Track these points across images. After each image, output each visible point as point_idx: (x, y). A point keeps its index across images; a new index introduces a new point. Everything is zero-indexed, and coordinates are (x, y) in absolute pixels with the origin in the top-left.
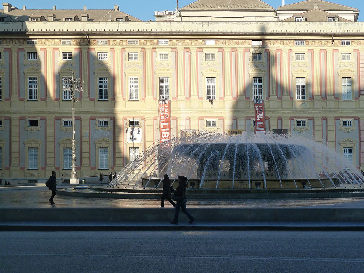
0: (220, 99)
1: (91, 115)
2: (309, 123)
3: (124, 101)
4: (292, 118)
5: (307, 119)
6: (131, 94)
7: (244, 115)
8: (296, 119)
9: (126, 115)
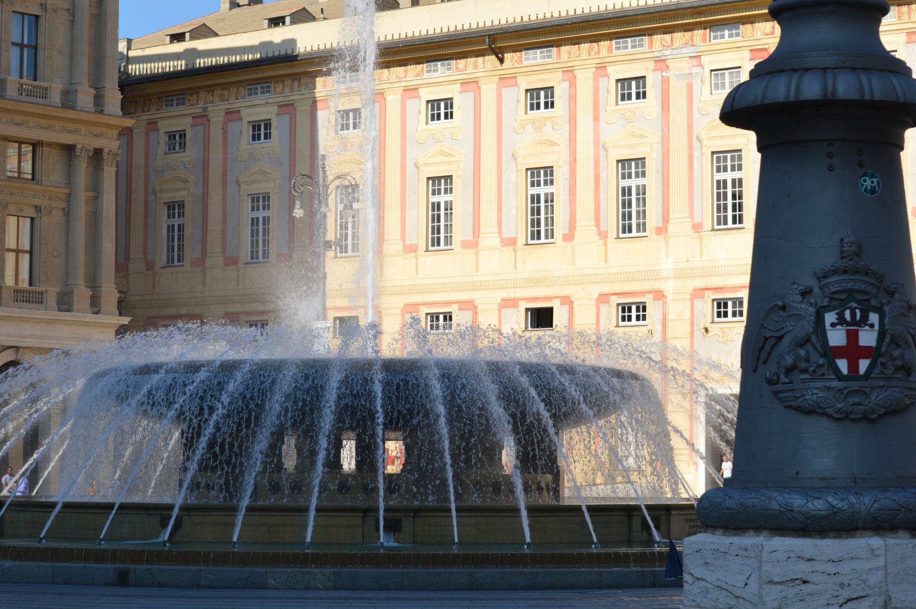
1: (504, 294)
3: (602, 242)
6: (627, 216)
9: (607, 288)
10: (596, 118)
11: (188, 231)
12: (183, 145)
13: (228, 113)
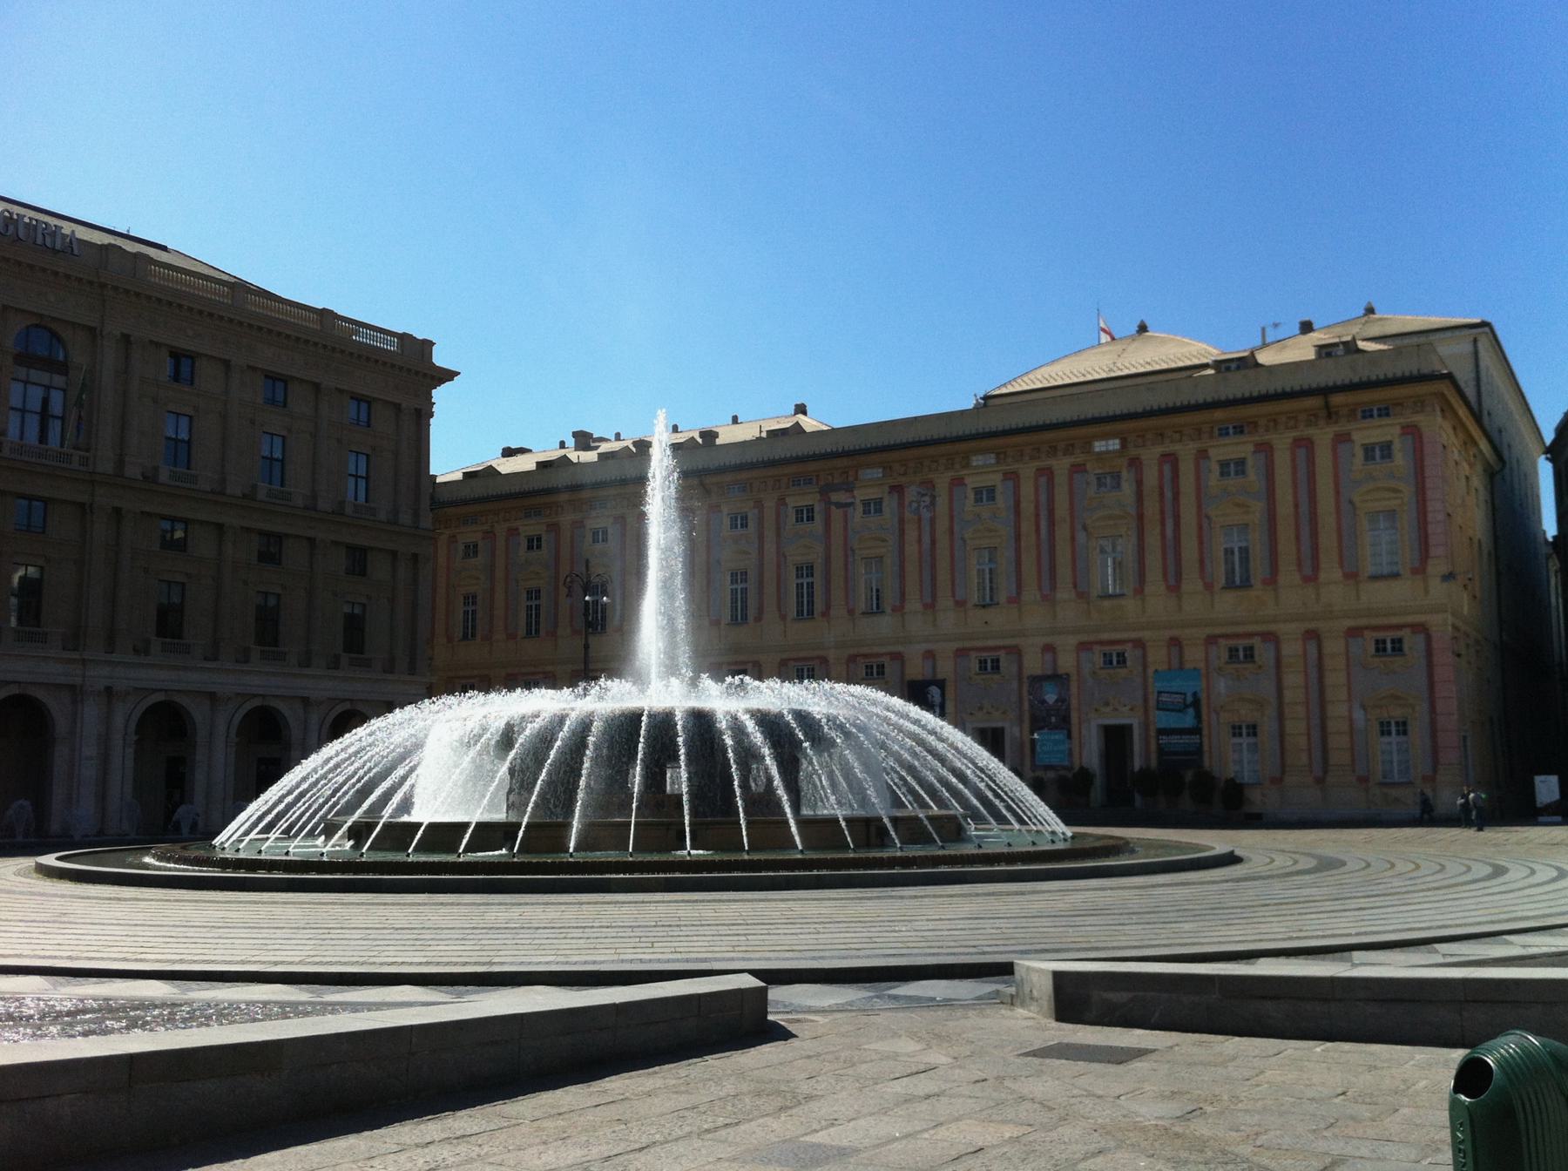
0: (1011, 601)
2: (1265, 654)
4: (1211, 640)
5: (1256, 642)
7: (1072, 640)
8: (1222, 642)
10: (778, 535)
11: (479, 615)
12: (476, 553)
13: (509, 530)
